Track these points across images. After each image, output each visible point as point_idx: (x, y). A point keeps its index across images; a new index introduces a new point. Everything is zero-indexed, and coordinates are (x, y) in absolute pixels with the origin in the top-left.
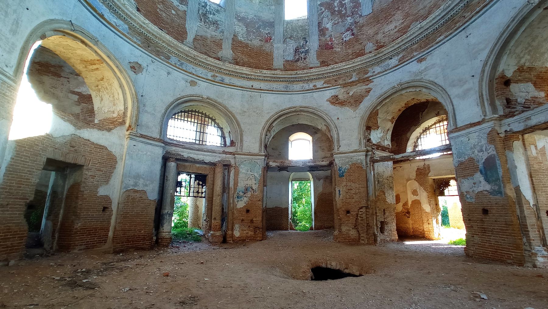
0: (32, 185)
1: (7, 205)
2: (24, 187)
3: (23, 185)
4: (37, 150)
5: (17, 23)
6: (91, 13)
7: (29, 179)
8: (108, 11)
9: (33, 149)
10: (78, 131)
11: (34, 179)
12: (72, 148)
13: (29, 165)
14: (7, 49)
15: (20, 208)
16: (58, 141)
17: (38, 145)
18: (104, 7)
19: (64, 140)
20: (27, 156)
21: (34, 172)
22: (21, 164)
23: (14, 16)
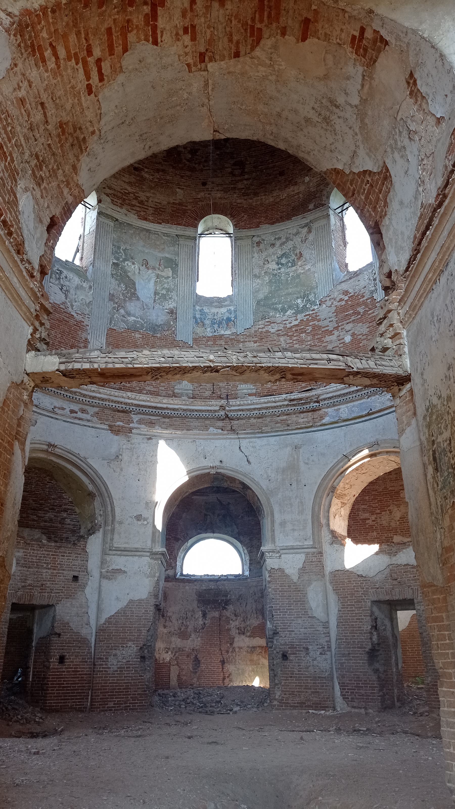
0: (365, 633)
1: (349, 654)
2: (358, 636)
3: (357, 633)
4: (359, 597)
5: (302, 503)
6: (363, 421)
7: (361, 627)
8: (377, 396)
9: (355, 597)
10: (394, 558)
11: (366, 627)
12: (394, 581)
13: (356, 613)
14: (302, 528)
15: (362, 657)
16: (378, 579)
17: (357, 591)
18: (373, 398)
19: (383, 576)
20: (351, 605)
21: (362, 619)
22: (348, 614)
23: (298, 500)
